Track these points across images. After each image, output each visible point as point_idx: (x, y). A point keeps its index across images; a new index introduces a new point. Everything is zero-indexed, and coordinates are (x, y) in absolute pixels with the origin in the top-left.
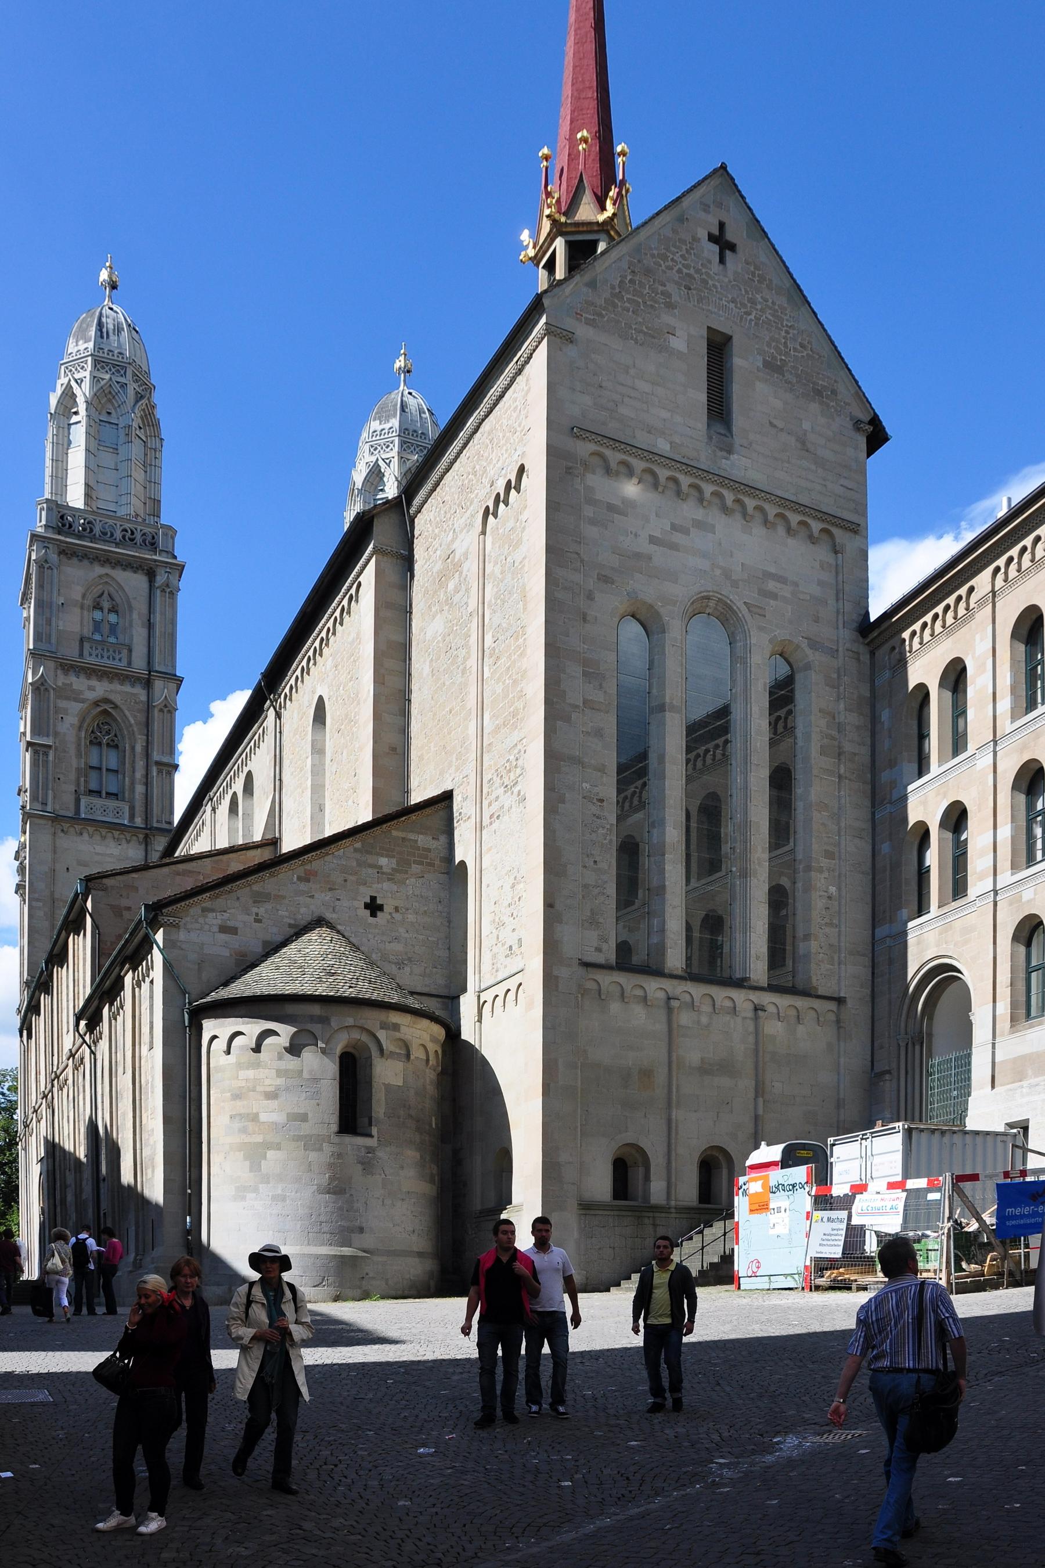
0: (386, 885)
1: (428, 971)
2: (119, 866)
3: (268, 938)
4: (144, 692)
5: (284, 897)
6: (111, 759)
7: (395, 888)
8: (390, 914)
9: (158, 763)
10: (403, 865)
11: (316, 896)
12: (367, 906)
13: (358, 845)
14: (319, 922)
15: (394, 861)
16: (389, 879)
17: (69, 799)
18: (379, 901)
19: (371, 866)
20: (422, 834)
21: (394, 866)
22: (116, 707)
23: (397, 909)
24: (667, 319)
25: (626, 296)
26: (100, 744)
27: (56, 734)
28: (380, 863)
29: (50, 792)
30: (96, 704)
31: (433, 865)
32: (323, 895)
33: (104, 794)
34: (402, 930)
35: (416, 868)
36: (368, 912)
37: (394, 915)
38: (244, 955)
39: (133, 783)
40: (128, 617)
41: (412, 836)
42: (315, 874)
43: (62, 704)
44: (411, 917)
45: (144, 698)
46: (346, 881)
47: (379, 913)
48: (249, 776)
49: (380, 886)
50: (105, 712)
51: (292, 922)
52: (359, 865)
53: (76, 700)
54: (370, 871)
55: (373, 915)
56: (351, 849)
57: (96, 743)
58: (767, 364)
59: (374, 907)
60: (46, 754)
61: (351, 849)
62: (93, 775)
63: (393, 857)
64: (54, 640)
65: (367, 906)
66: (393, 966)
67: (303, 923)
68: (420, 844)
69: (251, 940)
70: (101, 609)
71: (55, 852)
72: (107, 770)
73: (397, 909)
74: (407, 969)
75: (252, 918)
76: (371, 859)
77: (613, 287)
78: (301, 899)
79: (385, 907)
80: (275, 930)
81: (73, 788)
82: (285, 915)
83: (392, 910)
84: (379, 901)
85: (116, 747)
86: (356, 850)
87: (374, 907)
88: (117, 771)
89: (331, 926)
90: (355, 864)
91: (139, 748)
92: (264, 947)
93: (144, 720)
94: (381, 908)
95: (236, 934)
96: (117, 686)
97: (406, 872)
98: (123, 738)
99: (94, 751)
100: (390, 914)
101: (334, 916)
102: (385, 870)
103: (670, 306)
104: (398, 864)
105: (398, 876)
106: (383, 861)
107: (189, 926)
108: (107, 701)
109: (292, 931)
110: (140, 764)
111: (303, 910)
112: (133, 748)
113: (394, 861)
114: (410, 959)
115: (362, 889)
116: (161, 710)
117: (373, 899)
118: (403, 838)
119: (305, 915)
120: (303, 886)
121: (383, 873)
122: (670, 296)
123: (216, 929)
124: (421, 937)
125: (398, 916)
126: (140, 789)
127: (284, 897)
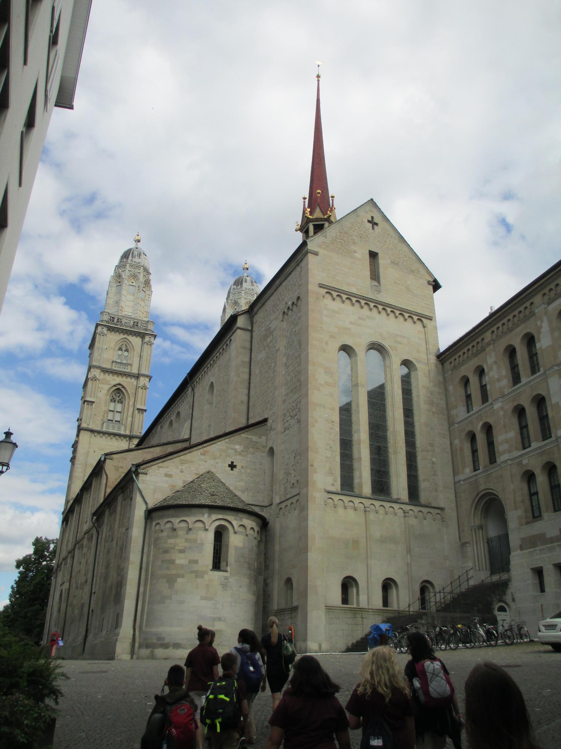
0: (238, 457)
2: (120, 449)
4: (136, 382)
6: (119, 407)
9: (138, 409)
15: (242, 447)
16: (240, 455)
17: (100, 423)
18: (235, 464)
19: (232, 449)
22: (123, 387)
24: (353, 248)
25: (338, 240)
26: (115, 401)
27: (97, 397)
29: (91, 420)
30: (115, 386)
33: (114, 421)
38: (174, 487)
39: (127, 416)
40: (132, 354)
43: (101, 386)
45: (135, 384)
47: (234, 469)
48: (179, 413)
50: (119, 389)
53: (107, 384)
54: (232, 451)
57: (113, 400)
58: (392, 262)
59: (232, 466)
60: (92, 405)
62: (111, 413)
63: (242, 445)
64: (101, 362)
70: (122, 350)
71: (90, 444)
72: (117, 412)
73: (242, 467)
75: (179, 471)
77: (333, 237)
79: (237, 467)
81: (101, 418)
84: (235, 464)
85: (122, 402)
87: (232, 466)
88: (120, 412)
91: (131, 403)
93: (134, 392)
94: (235, 466)
96: (124, 379)
98: (125, 399)
99: (112, 404)
102: (238, 451)
103: (355, 243)
106: (237, 447)
108: (119, 384)
110: (131, 409)
112: (129, 403)
113: (242, 447)
116: (142, 388)
117: (232, 462)
121: (237, 452)
122: (354, 240)
125: (243, 470)
126: (130, 419)
127: (193, 462)
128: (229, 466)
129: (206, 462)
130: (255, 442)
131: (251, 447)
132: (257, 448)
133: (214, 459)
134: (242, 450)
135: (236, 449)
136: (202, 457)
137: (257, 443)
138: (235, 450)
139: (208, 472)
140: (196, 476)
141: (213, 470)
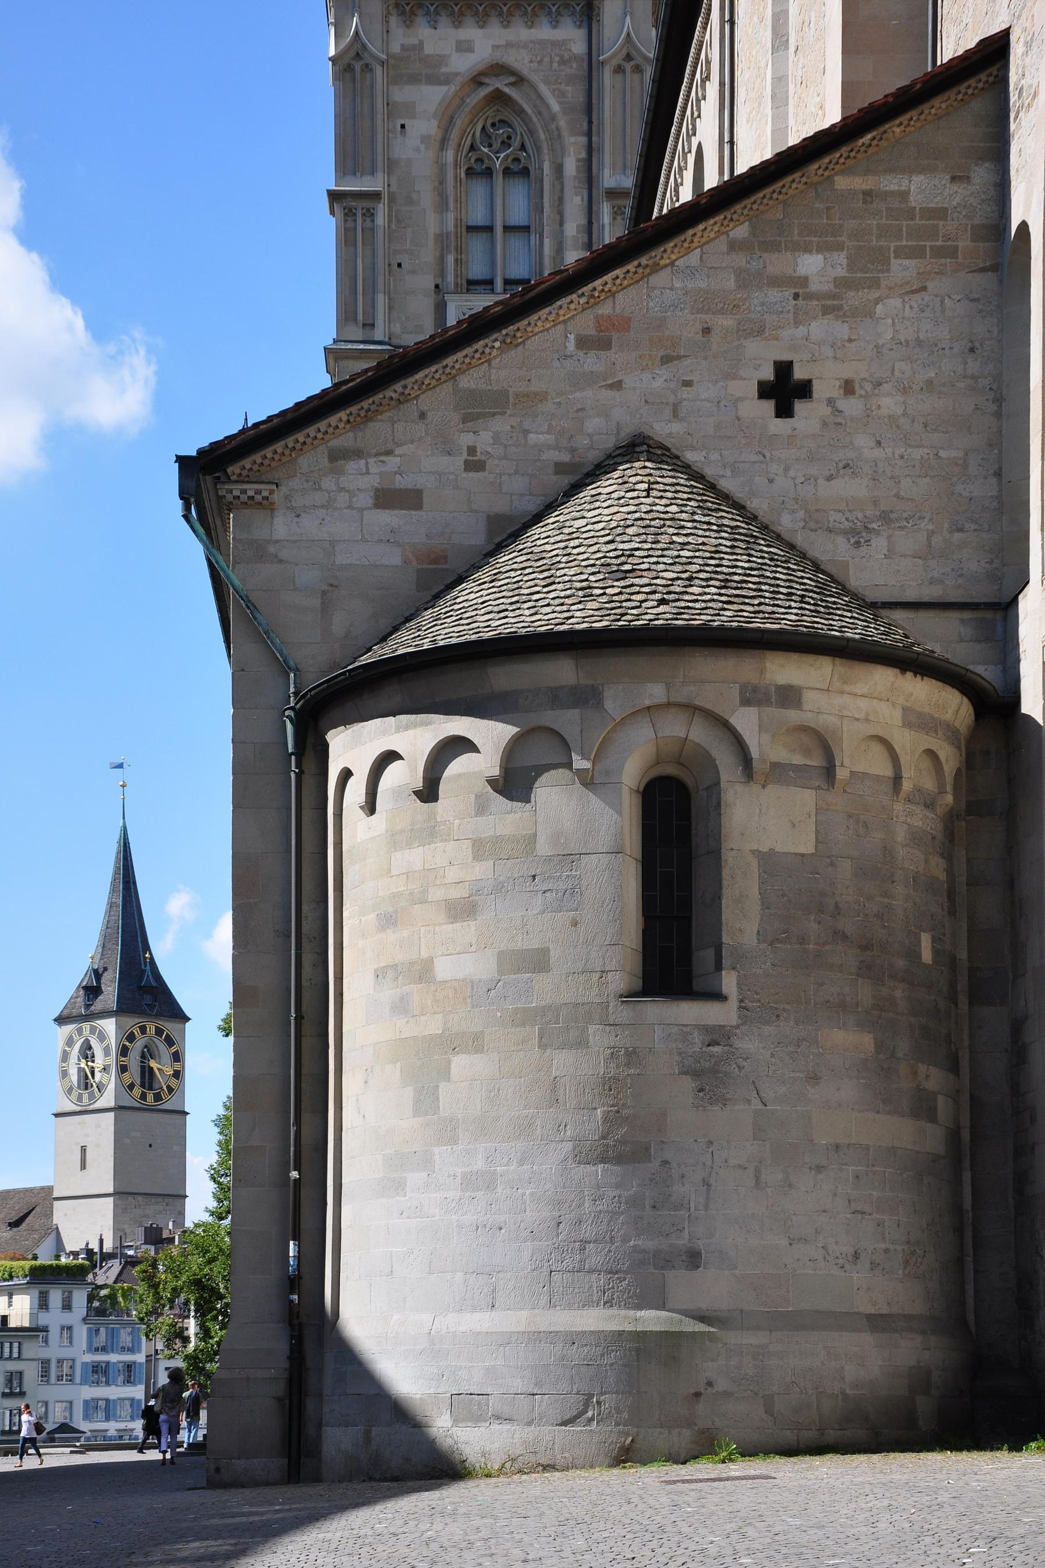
0: (818, 328)
1: (937, 540)
3: (501, 506)
5: (541, 397)
7: (842, 330)
8: (830, 402)
10: (867, 267)
11: (629, 381)
12: (765, 391)
13: (741, 232)
14: (636, 447)
16: (826, 311)
18: (799, 374)
19: (776, 282)
20: (921, 171)
21: (841, 272)
23: (848, 388)
28: (802, 271)
31: (953, 253)
32: (646, 376)
34: (863, 442)
35: (902, 269)
36: (768, 406)
37: (841, 404)
42: (624, 324)
44: (889, 404)
46: (707, 331)
49: (802, 330)
51: (565, 457)
52: (746, 280)
54: (774, 295)
55: (784, 411)
56: (722, 244)
59: (785, 391)
61: (722, 244)
63: (839, 247)
65: (765, 391)
66: (840, 540)
67: (594, 456)
68: (915, 200)
69: (454, 514)
73: (848, 388)
74: (880, 544)
76: (776, 263)
78: (588, 395)
79: (817, 387)
80: (518, 484)
82: (545, 440)
83: (836, 393)
86: (734, 246)
87: (785, 391)
89: (661, 454)
90: (731, 283)
92: (490, 533)
94: (804, 390)
95: (418, 506)
97: (875, 283)
100: (830, 402)
101: (676, 427)
102: (814, 287)
104: (851, 267)
105: (853, 299)
106: (809, 264)
107: (298, 501)
109: (565, 481)
111: (594, 424)
114: (885, 517)
115: (753, 347)
117: (784, 369)
118: (868, 195)
119: (598, 433)
120: (592, 362)
121: (809, 297)
123: (365, 500)
125: (851, 407)
134: (838, 282)
135: (804, 281)
138: (799, 287)
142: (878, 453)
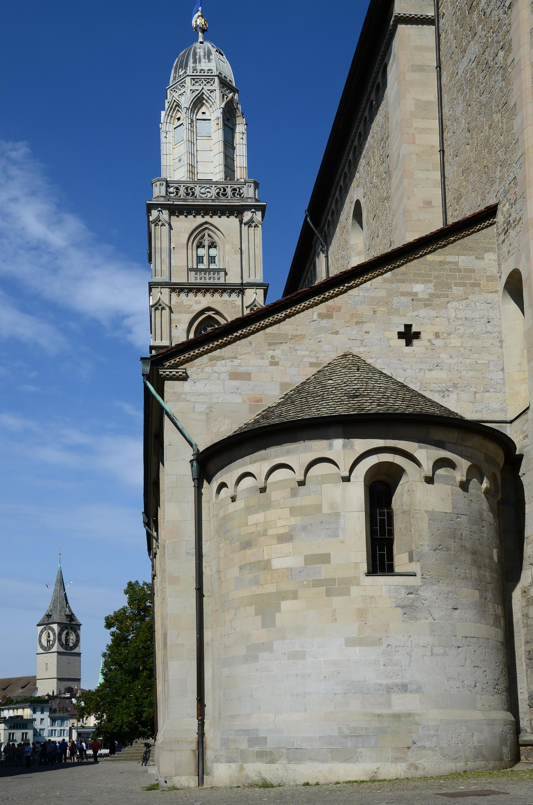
0: (423, 312)
7: (434, 313)
8: (429, 340)
16: (426, 306)
18: (414, 329)
21: (433, 291)
37: (434, 341)
41: (449, 258)
49: (416, 313)
59: (409, 335)
83: (432, 337)
84: (414, 329)
87: (409, 335)
100: (429, 340)
102: (420, 296)
106: (418, 288)
117: (408, 327)
124: (468, 361)
125: (438, 343)
128: (401, 335)
129: (337, 333)
130: (466, 270)
131: (456, 285)
132: (473, 285)
133: (357, 323)
135: (416, 294)
136: (324, 323)
137: (473, 271)
138: (414, 296)
139: (345, 356)
140: (315, 370)
141: (355, 351)
142: (450, 361)
